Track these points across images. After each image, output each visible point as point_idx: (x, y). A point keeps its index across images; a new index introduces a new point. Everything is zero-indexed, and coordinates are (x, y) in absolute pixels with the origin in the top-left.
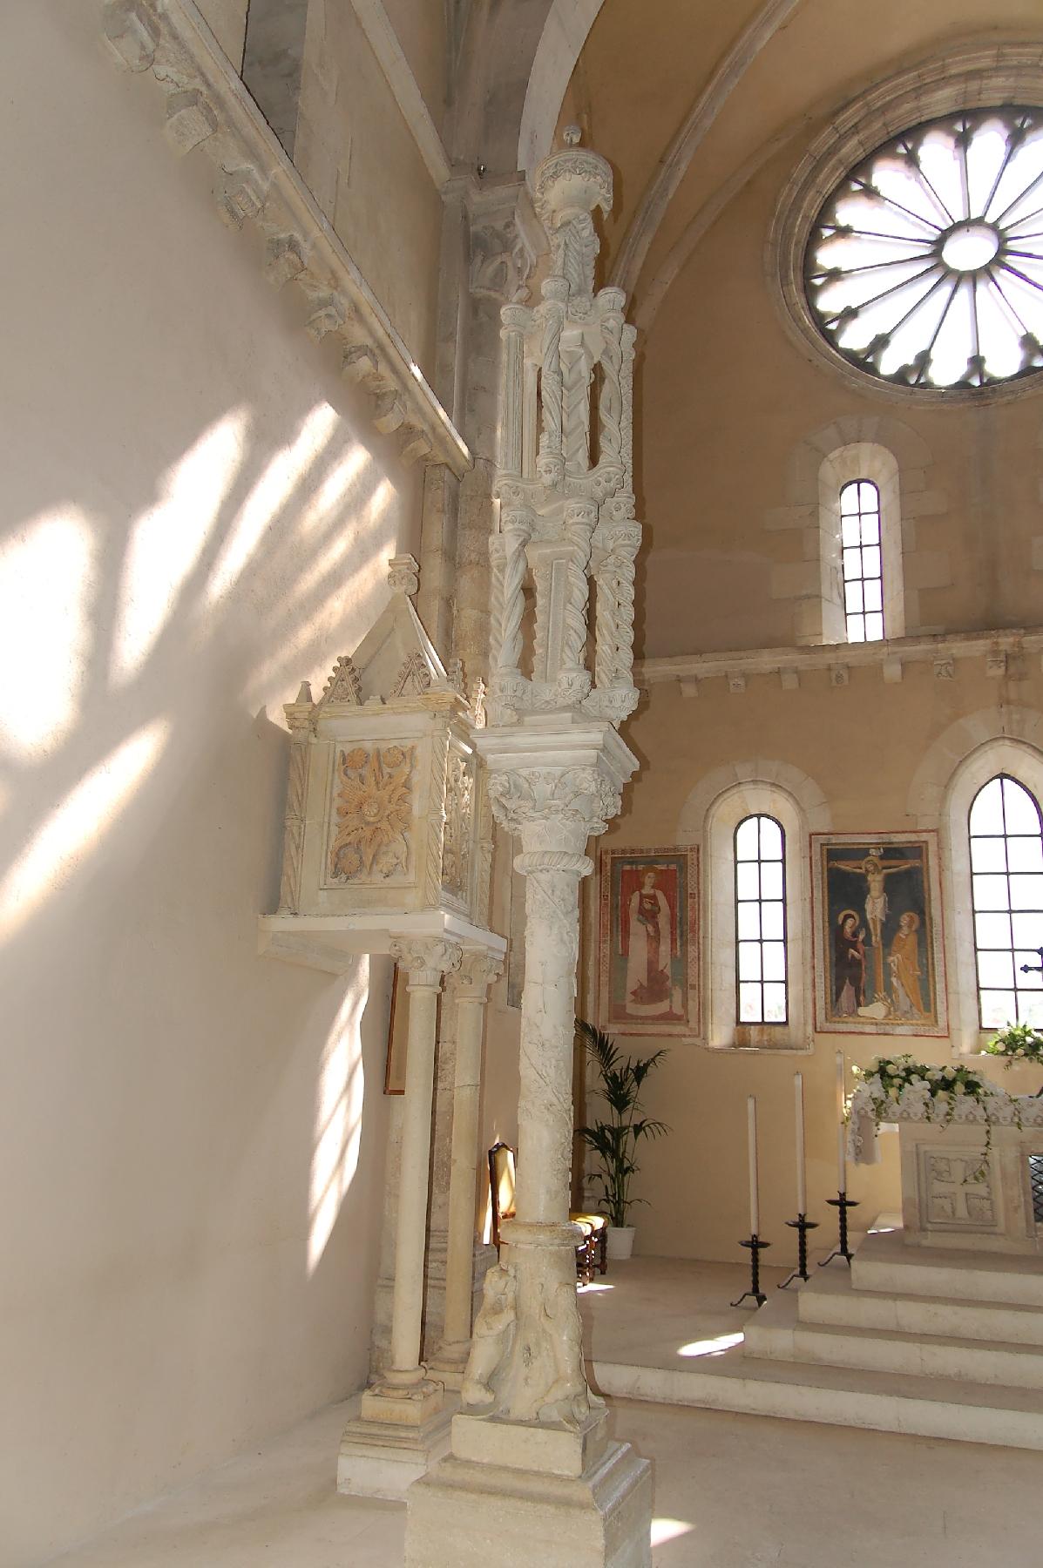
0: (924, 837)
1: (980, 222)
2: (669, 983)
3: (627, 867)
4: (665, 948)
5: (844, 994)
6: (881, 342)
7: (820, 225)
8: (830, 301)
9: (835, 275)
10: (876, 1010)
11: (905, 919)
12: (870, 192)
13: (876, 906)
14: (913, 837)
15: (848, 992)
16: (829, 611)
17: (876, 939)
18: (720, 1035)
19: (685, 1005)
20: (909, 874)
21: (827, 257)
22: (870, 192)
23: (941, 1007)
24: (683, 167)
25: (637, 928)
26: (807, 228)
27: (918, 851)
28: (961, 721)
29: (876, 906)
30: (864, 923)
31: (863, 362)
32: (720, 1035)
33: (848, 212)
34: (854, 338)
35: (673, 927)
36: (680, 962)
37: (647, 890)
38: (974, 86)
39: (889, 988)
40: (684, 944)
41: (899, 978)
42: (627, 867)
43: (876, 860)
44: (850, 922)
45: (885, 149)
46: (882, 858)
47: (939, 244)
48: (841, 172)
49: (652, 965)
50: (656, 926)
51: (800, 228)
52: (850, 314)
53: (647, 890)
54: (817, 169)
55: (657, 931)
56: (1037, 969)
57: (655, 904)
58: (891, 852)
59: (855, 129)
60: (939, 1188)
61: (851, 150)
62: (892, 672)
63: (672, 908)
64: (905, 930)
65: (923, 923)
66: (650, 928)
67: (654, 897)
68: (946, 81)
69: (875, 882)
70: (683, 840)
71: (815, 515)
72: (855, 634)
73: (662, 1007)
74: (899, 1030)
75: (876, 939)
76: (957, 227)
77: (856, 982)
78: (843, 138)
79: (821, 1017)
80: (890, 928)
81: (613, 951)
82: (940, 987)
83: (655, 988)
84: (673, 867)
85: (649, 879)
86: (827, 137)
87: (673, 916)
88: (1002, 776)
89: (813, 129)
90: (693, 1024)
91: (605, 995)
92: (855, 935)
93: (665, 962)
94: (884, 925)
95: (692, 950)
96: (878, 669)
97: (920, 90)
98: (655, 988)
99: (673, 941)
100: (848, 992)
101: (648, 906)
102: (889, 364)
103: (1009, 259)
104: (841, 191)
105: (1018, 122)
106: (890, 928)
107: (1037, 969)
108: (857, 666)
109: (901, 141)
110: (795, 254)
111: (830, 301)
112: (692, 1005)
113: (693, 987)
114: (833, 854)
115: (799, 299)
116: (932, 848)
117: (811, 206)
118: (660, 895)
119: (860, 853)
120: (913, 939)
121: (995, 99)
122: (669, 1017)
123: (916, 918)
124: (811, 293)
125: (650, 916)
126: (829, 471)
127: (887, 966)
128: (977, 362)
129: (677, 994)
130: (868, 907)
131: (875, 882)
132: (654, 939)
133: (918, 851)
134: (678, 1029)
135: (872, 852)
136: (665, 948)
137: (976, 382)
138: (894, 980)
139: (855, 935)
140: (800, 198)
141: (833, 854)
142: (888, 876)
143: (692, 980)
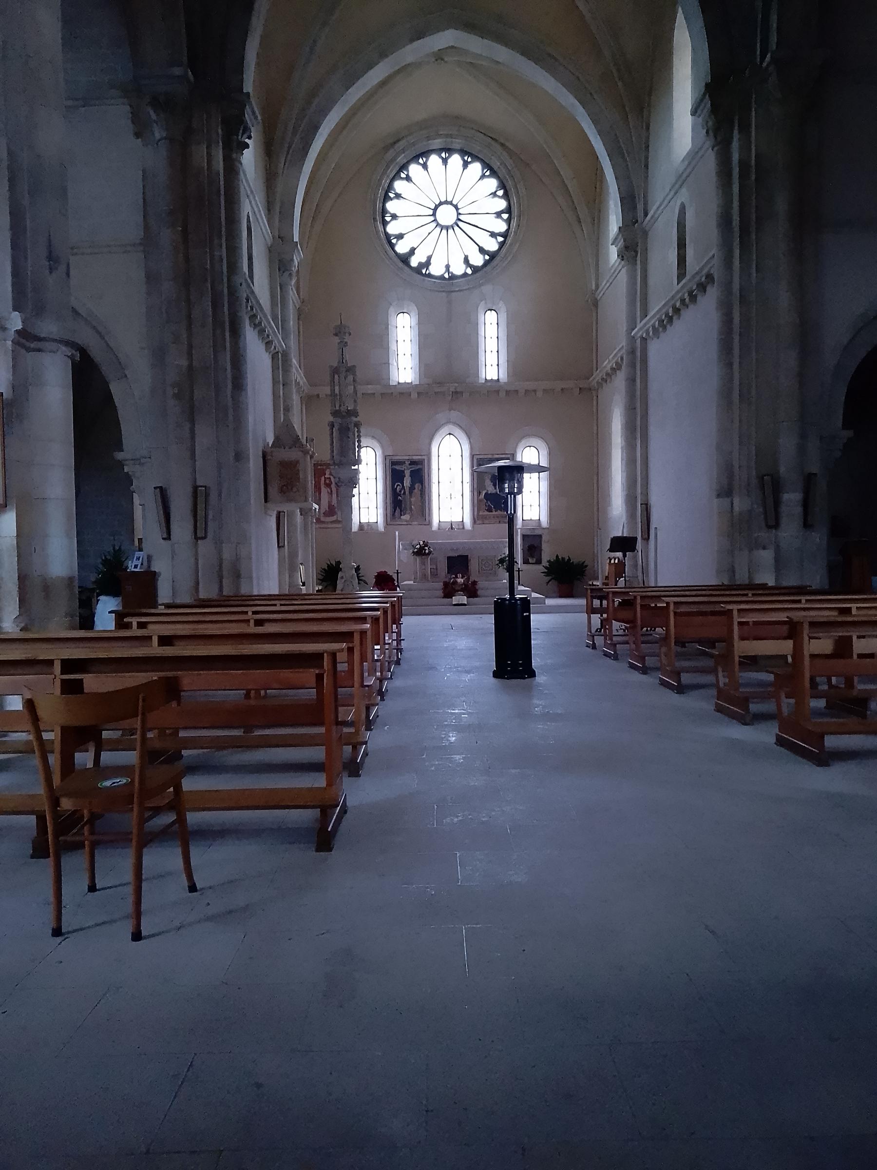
1: (451, 203)
4: (334, 496)
6: (412, 251)
8: (393, 228)
10: (406, 517)
12: (408, 179)
13: (407, 482)
17: (407, 493)
18: (355, 527)
21: (391, 206)
22: (408, 179)
26: (384, 192)
27: (421, 462)
29: (407, 482)
31: (405, 259)
32: (355, 527)
34: (402, 248)
38: (449, 140)
39: (411, 509)
45: (415, 159)
47: (435, 210)
48: (397, 168)
51: (381, 193)
52: (400, 236)
54: (388, 167)
58: (413, 463)
59: (403, 151)
61: (401, 160)
62: (414, 395)
64: (416, 491)
68: (439, 136)
69: (407, 473)
71: (387, 328)
73: (334, 518)
75: (407, 493)
76: (441, 204)
78: (398, 155)
80: (412, 488)
85: (327, 472)
86: (391, 153)
89: (386, 149)
93: (334, 502)
97: (428, 138)
98: (331, 511)
100: (398, 510)
101: (328, 482)
102: (414, 262)
103: (460, 224)
104: (396, 176)
105: (466, 158)
106: (412, 488)
110: (379, 205)
111: (393, 228)
114: (393, 463)
115: (381, 228)
116: (426, 461)
117: (385, 183)
121: (458, 147)
124: (385, 223)
126: (392, 310)
127: (411, 502)
128: (448, 267)
129: (339, 513)
131: (407, 473)
133: (421, 462)
136: (334, 496)
137: (446, 276)
140: (380, 180)
141: (393, 463)
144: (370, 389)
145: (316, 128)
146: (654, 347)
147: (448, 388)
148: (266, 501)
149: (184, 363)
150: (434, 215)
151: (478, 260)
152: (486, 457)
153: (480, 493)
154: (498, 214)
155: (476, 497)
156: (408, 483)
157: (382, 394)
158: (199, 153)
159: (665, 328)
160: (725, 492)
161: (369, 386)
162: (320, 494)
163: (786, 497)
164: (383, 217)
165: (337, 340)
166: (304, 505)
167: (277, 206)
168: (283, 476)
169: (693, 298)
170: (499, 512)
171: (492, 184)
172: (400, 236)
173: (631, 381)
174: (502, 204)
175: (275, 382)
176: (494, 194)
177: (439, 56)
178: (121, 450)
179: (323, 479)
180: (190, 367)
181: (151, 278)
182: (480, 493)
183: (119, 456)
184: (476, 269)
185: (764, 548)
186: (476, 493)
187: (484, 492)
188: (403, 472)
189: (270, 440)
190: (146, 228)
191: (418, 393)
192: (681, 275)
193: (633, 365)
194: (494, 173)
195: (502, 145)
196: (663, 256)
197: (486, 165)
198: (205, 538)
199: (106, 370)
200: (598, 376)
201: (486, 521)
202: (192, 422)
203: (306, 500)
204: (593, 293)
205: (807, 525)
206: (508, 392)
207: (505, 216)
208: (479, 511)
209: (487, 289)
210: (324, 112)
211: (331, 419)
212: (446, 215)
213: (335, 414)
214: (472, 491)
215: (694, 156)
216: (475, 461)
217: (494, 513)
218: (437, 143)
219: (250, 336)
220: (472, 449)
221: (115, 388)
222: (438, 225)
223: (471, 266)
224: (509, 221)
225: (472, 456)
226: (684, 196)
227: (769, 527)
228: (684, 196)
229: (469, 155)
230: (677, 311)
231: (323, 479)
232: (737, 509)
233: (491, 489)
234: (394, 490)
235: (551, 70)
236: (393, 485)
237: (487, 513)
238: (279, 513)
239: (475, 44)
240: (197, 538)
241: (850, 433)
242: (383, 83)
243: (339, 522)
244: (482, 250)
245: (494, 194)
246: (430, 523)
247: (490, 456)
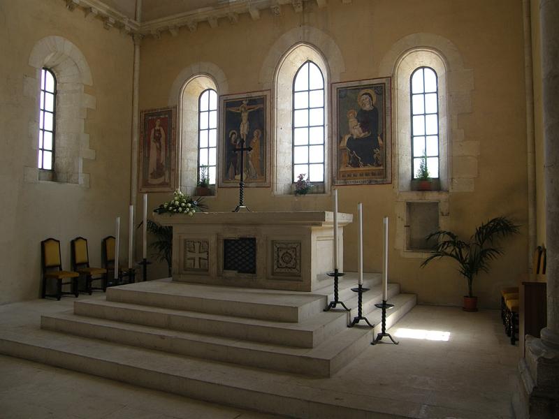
0: (265, 93)
2: (164, 169)
3: (150, 118)
4: (163, 153)
5: (230, 170)
11: (255, 133)
13: (244, 129)
14: (260, 94)
19: (170, 178)
20: (258, 111)
23: (268, 174)
25: (153, 145)
28: (284, 35)
29: (244, 129)
30: (239, 136)
35: (166, 144)
36: (168, 159)
37: (157, 128)
40: (170, 151)
41: (252, 161)
42: (150, 118)
43: (245, 106)
44: (234, 136)
46: (247, 104)
49: (158, 160)
50: (160, 143)
53: (157, 128)
55: (160, 146)
56: (50, 132)
57: (160, 134)
58: (252, 101)
60: (190, 255)
63: (166, 135)
64: (255, 138)
65: (263, 133)
66: (158, 144)
67: (159, 130)
69: (245, 116)
70: (170, 104)
73: (161, 180)
74: (250, 185)
77: (235, 164)
79: (221, 179)
80: (250, 136)
81: (144, 156)
82: (268, 164)
83: (159, 172)
84: (167, 116)
85: (158, 123)
87: (166, 138)
88: (309, 61)
90: (173, 187)
91: (141, 178)
92: (235, 142)
94: (247, 136)
95: (173, 153)
96: (248, 14)
98: (159, 172)
99: (166, 150)
106: (250, 136)
107: (50, 132)
112: (172, 178)
113: (173, 170)
116: (268, 98)
118: (162, 129)
120: (258, 142)
122: (164, 184)
123: (260, 132)
125: (158, 139)
129: (167, 173)
130: (241, 129)
131: (245, 116)
132: (159, 149)
133: (262, 100)
134: (167, 189)
135: (244, 102)
136: (163, 153)
138: (250, 162)
139: (235, 142)
142: (249, 115)
143: (173, 167)
152: (350, 84)
155: (335, 146)
161: (200, 10)
162: (149, 150)
170: (370, 168)
179: (153, 132)
182: (340, 139)
186: (335, 139)
187: (347, 138)
188: (240, 114)
191: (261, 11)
201: (351, 182)
208: (339, 167)
216: (335, 92)
217: (362, 168)
220: (329, 74)
225: (331, 85)
231: (153, 132)
233: (357, 132)
236: (227, 135)
237: (350, 169)
243: (167, 184)
246: (270, 186)
247: (356, 84)
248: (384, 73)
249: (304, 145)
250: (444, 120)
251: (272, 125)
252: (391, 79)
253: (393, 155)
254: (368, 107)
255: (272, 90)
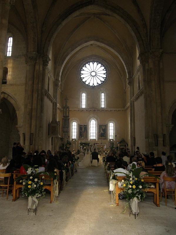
6: (86, 81)
7: (81, 69)
9: (82, 74)
10: (83, 138)
15: (81, 137)
16: (81, 105)
17: (83, 132)
24: (70, 64)
33: (84, 68)
52: (83, 78)
54: (81, 64)
58: (84, 125)
72: (83, 107)
75: (83, 132)
76: (92, 71)
106: (84, 131)
108: (83, 110)
109: (88, 62)
111: (82, 76)
119: (82, 125)
126: (81, 93)
128: (93, 84)
133: (86, 125)
144: (75, 109)
145: (65, 59)
146: (136, 103)
147: (93, 109)
148: (49, 135)
149: (31, 108)
150: (91, 73)
151: (100, 83)
153: (99, 133)
154: (104, 74)
156: (83, 130)
157: (78, 110)
158: (37, 67)
159: (137, 100)
160: (147, 137)
163: (159, 139)
164: (80, 74)
165: (65, 101)
166: (56, 136)
167: (56, 74)
168: (52, 128)
169: (141, 95)
171: (103, 68)
172: (83, 78)
173: (131, 110)
174: (105, 72)
175: (53, 109)
176: (103, 70)
177: (91, 45)
178: (17, 125)
180: (32, 109)
181: (26, 91)
182: (99, 133)
183: (17, 126)
184: (99, 85)
185: (155, 150)
187: (100, 133)
189: (51, 121)
190: (26, 81)
192: (139, 89)
193: (131, 106)
194: (103, 66)
195: (105, 60)
196: (136, 85)
197: (102, 64)
198: (32, 145)
199: (16, 109)
200: (126, 108)
202: (31, 119)
203: (57, 135)
204: (125, 90)
205: (164, 146)
206: (106, 110)
207: (106, 74)
208: (99, 136)
209: (102, 89)
210: (67, 55)
211: (63, 118)
212: (93, 74)
213: (64, 116)
214: (98, 132)
215: (140, 66)
216: (99, 125)
218: (92, 60)
219: (46, 100)
220: (98, 123)
221: (17, 112)
222: (91, 76)
223: (99, 84)
224: (106, 75)
225: (98, 124)
226: (139, 74)
227: (156, 146)
228: (139, 74)
229: (98, 62)
230: (139, 97)
232: (149, 141)
233: (102, 132)
234: (80, 132)
235: (113, 49)
236: (80, 130)
238: (52, 138)
239: (98, 43)
240: (30, 145)
241: (173, 125)
242: (80, 49)
244: (101, 81)
245: (103, 70)
246: (88, 139)
248: (106, 123)
249: (93, 133)
250: (114, 131)
251: (88, 130)
252: (107, 124)
253: (107, 136)
254: (104, 128)
255: (88, 124)
